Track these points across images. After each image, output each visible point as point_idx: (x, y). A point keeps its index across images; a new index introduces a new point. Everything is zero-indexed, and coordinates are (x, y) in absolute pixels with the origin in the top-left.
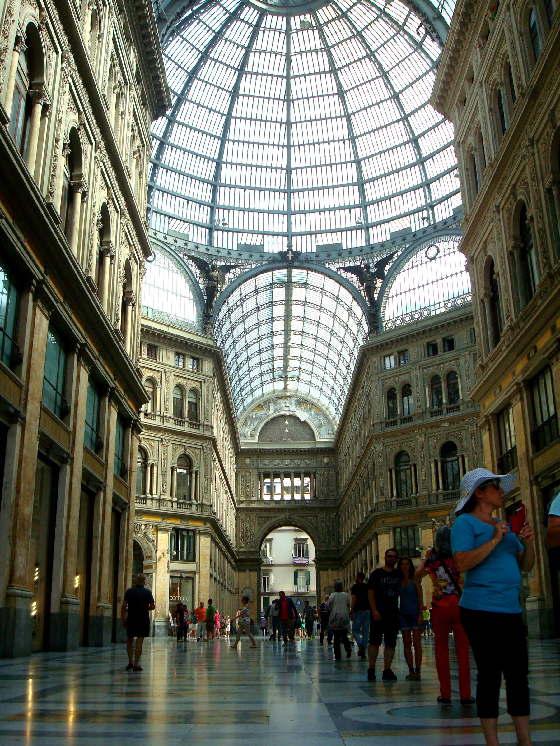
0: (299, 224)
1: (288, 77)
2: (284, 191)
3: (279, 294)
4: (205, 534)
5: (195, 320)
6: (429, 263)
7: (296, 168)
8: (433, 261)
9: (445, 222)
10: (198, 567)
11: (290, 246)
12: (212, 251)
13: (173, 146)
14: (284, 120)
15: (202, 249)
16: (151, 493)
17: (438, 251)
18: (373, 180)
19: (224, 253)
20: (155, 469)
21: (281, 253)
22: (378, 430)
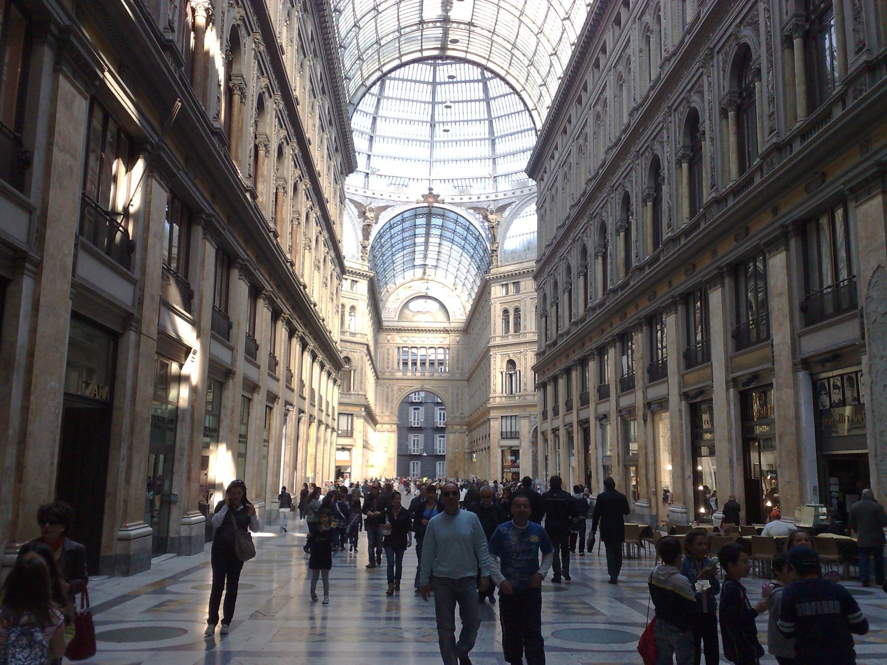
0: (439, 171)
2: (428, 142)
7: (439, 122)
11: (431, 189)
12: (369, 194)
14: (431, 80)
15: (361, 192)
18: (502, 137)
22: (492, 343)
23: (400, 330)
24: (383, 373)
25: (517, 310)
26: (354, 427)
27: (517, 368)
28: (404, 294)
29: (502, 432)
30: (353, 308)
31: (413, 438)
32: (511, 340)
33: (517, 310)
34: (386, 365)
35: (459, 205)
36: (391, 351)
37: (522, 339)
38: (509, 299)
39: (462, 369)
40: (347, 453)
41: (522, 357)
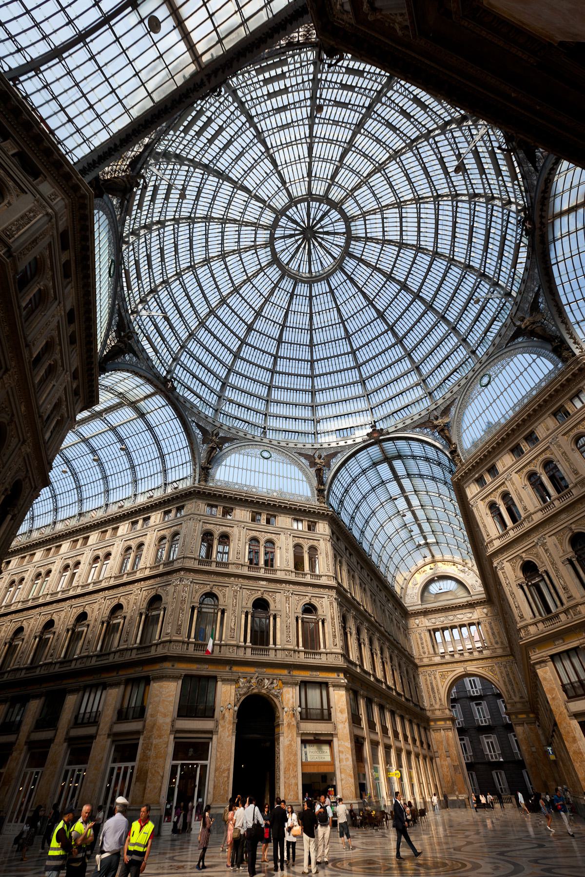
0: (380, 413)
1: (343, 322)
3: (384, 470)
4: (337, 686)
5: (310, 495)
6: (486, 390)
8: (489, 386)
9: (487, 353)
10: (335, 728)
13: (278, 388)
14: (350, 350)
16: (275, 643)
17: (490, 377)
19: (325, 446)
20: (278, 620)
21: (368, 435)
23: (425, 613)
24: (421, 659)
25: (506, 496)
26: (332, 704)
27: (541, 570)
28: (420, 579)
29: (563, 686)
30: (313, 550)
31: (485, 741)
32: (512, 534)
33: (506, 496)
34: (422, 650)
35: (403, 429)
36: (422, 635)
37: (527, 526)
38: (489, 489)
39: (502, 643)
40: (326, 748)
41: (541, 550)
